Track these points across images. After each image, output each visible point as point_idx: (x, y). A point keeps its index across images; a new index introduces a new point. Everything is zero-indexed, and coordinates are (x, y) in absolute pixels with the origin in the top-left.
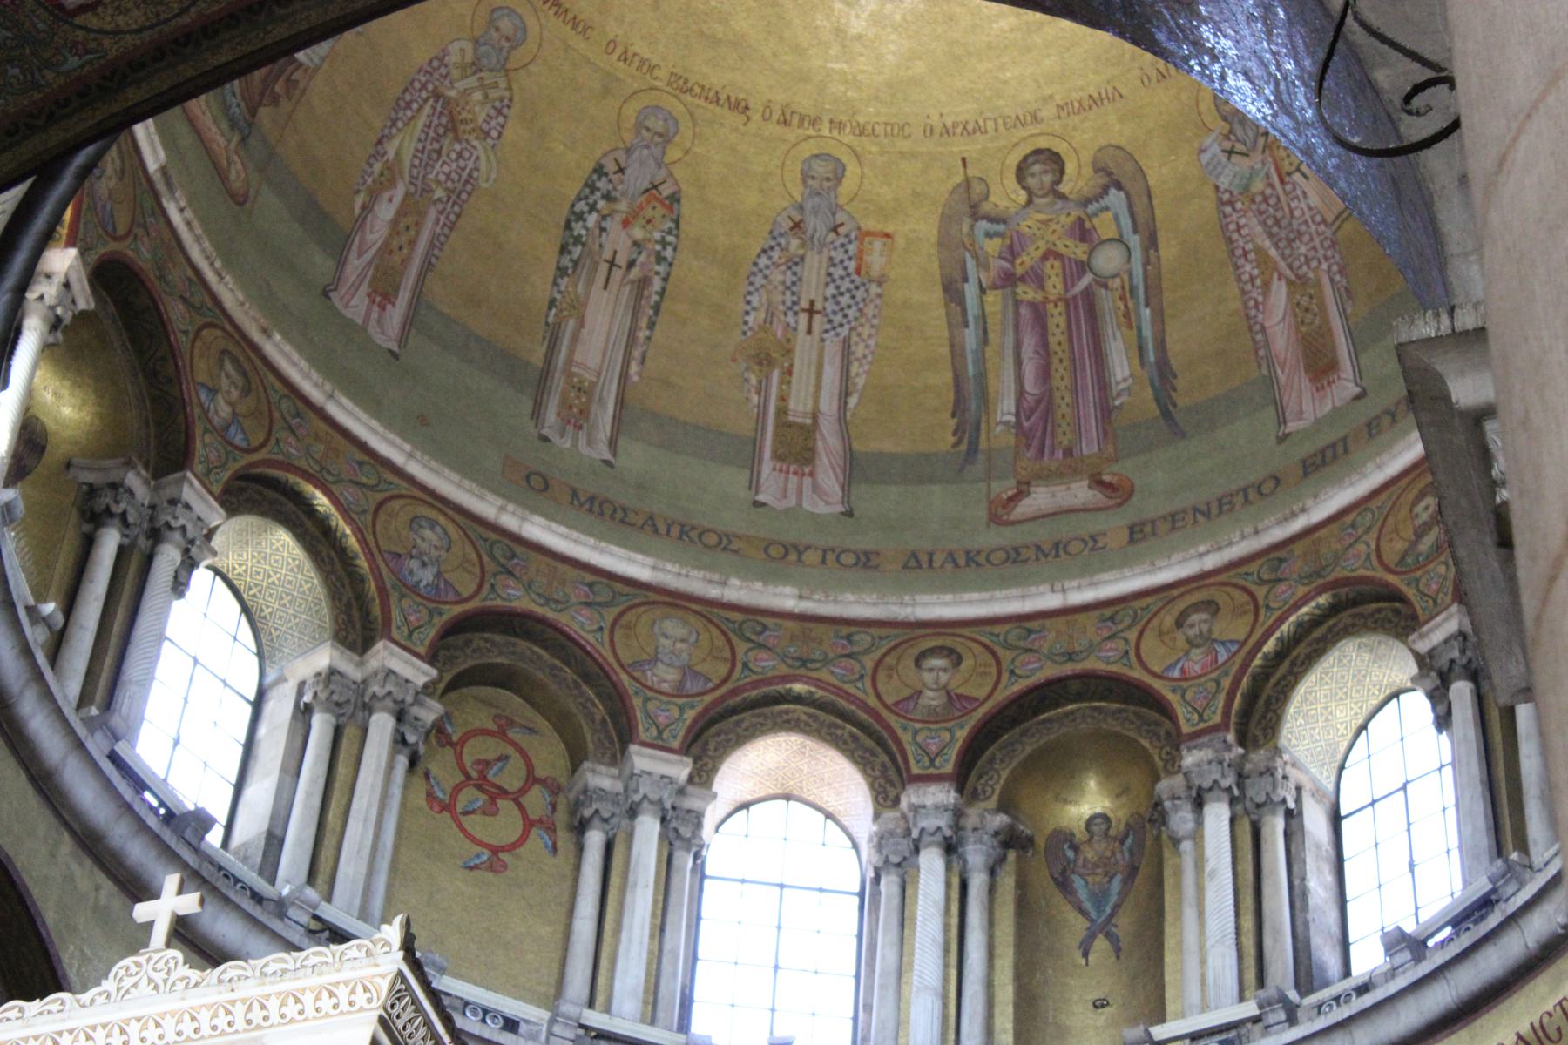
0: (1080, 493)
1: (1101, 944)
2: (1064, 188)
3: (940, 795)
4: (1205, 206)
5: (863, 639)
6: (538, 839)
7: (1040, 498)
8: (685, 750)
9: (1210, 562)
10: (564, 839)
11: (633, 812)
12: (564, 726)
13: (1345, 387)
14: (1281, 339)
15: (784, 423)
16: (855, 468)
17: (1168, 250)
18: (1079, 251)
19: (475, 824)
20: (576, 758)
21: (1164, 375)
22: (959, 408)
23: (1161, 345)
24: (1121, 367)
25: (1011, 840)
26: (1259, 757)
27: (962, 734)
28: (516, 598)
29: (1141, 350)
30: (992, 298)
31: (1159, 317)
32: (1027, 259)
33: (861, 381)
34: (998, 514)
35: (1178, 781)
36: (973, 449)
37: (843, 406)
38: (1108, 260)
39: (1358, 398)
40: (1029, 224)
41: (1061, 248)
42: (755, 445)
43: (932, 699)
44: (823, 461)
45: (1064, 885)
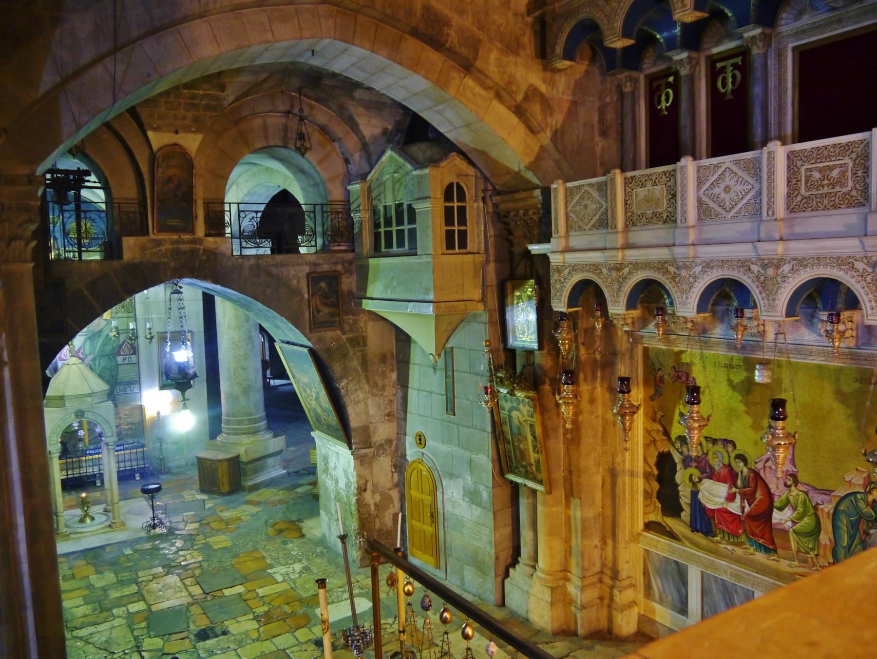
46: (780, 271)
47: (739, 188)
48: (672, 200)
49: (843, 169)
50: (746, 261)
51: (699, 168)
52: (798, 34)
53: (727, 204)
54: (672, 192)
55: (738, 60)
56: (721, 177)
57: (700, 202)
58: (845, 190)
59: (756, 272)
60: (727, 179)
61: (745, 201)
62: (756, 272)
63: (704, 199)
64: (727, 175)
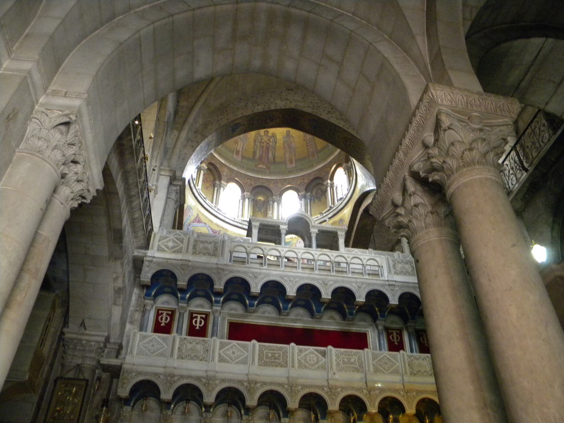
0: (264, 167)
1: (259, 212)
2: (268, 135)
3: (249, 194)
4: (282, 142)
5: (242, 175)
6: (210, 187)
7: (260, 166)
8: (226, 182)
9: (278, 178)
10: (213, 187)
11: (220, 187)
12: (213, 175)
13: (294, 165)
14: (287, 159)
15: (237, 150)
16: (243, 157)
17: (277, 145)
18: (268, 142)
19: (206, 184)
20: (214, 180)
21: (274, 158)
22: (253, 154)
23: (275, 153)
24: (270, 155)
25: (253, 200)
26: (280, 199)
27: (251, 188)
28: (214, 162)
29: (273, 154)
30: (259, 144)
31: (275, 151)
32: (263, 141)
33: (244, 148)
34: (256, 166)
35: (272, 199)
36: (254, 159)
37: (242, 150)
38: (271, 144)
39: (296, 167)
40: (264, 137)
41: (266, 141)
42: (234, 151)
43: (249, 183)
44: (240, 155)
45: (257, 205)
46: (256, 386)
47: (239, 353)
48: (206, 352)
49: (279, 355)
50: (242, 380)
51: (221, 343)
52: (231, 315)
53: (233, 358)
54: (206, 349)
55: (204, 316)
56: (232, 347)
57: (219, 354)
58: (279, 361)
59: (246, 385)
60: (234, 349)
61: (241, 358)
62: (246, 385)
63: (223, 354)
64: (234, 348)
